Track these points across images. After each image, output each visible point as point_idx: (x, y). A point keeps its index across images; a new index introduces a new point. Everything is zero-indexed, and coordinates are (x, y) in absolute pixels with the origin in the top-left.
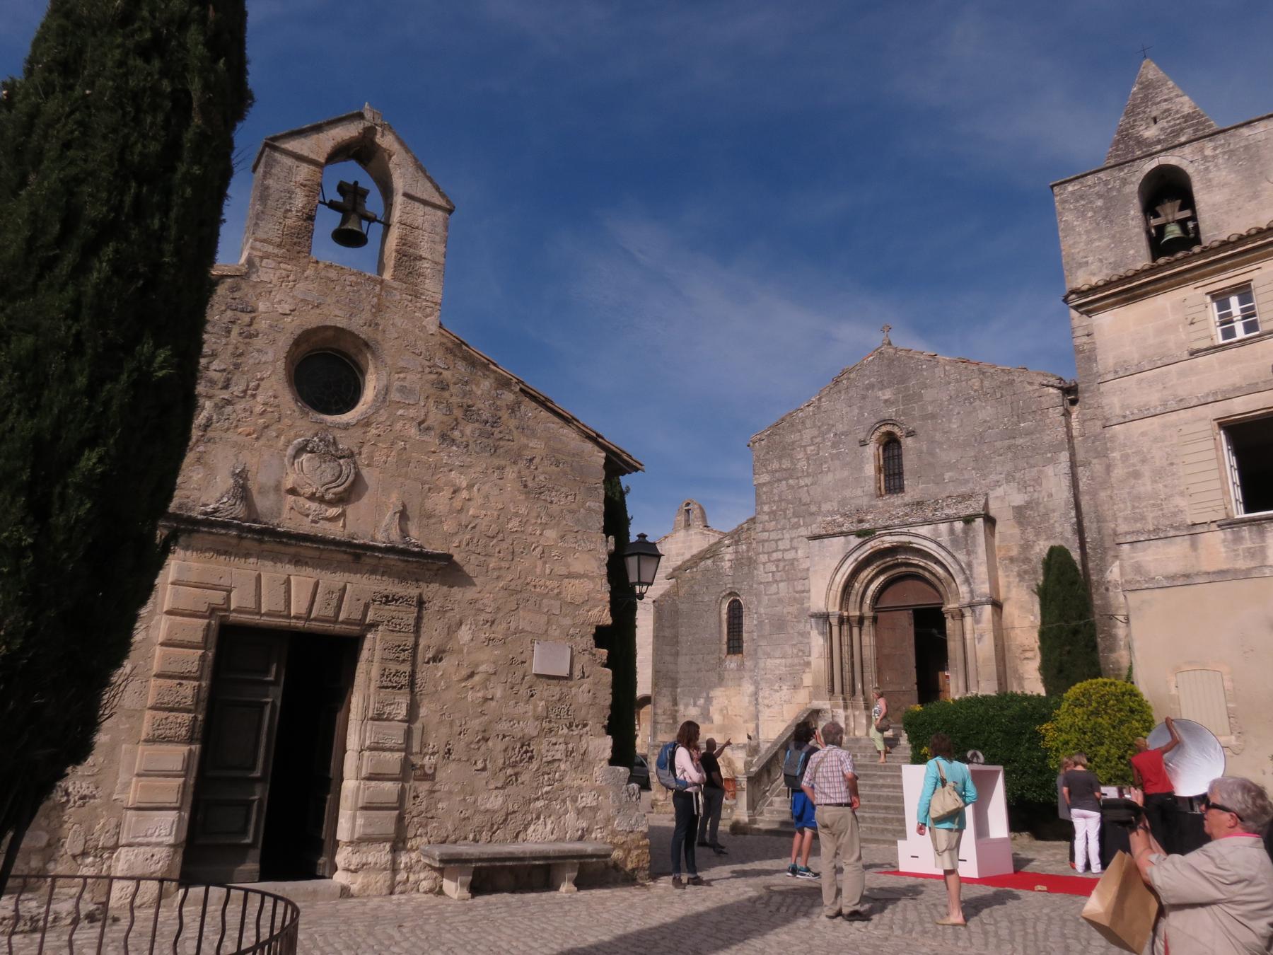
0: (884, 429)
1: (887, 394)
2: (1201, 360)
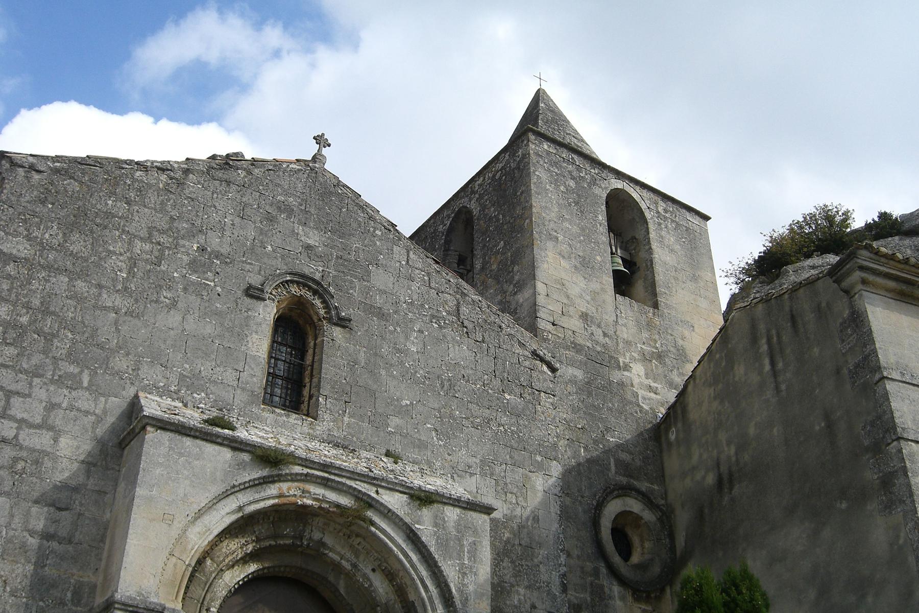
1: (314, 238)
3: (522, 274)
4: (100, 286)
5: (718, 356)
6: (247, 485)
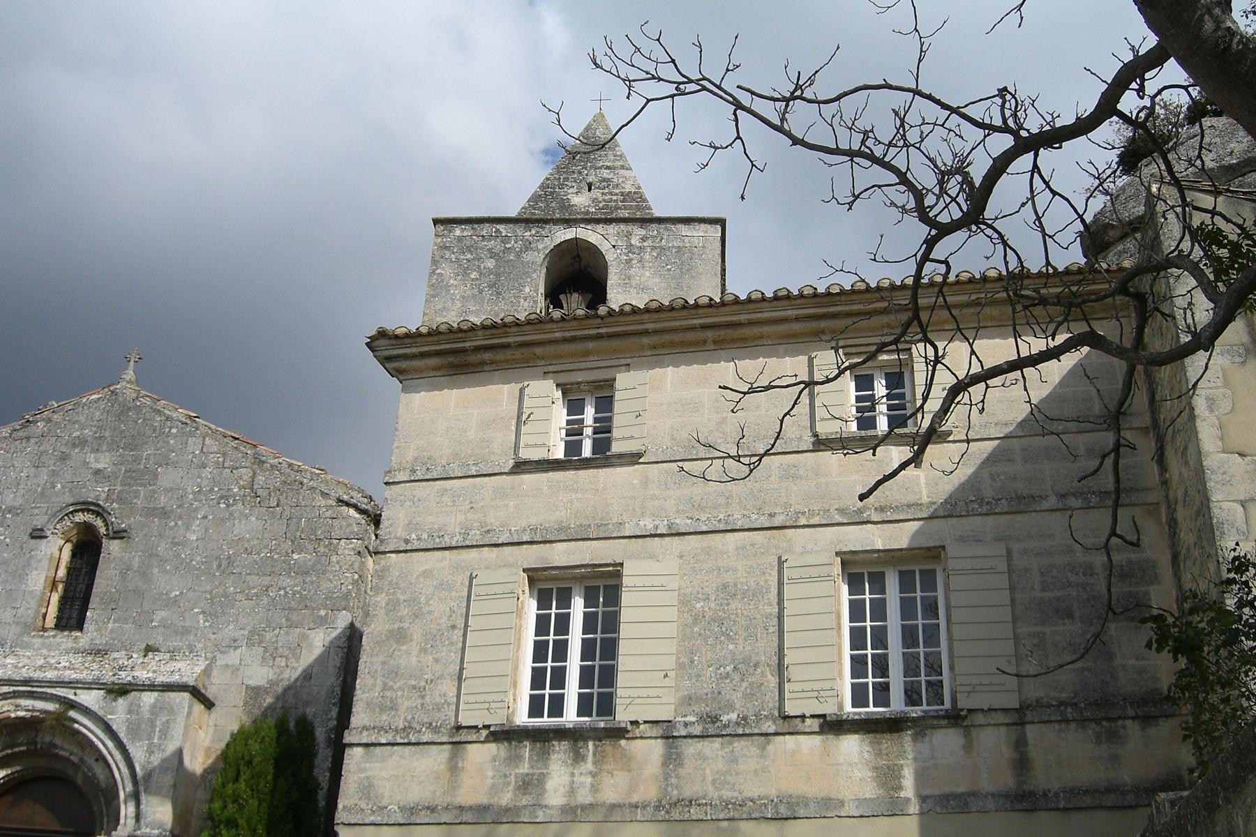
0: (80, 518)
1: (103, 461)
2: (529, 480)
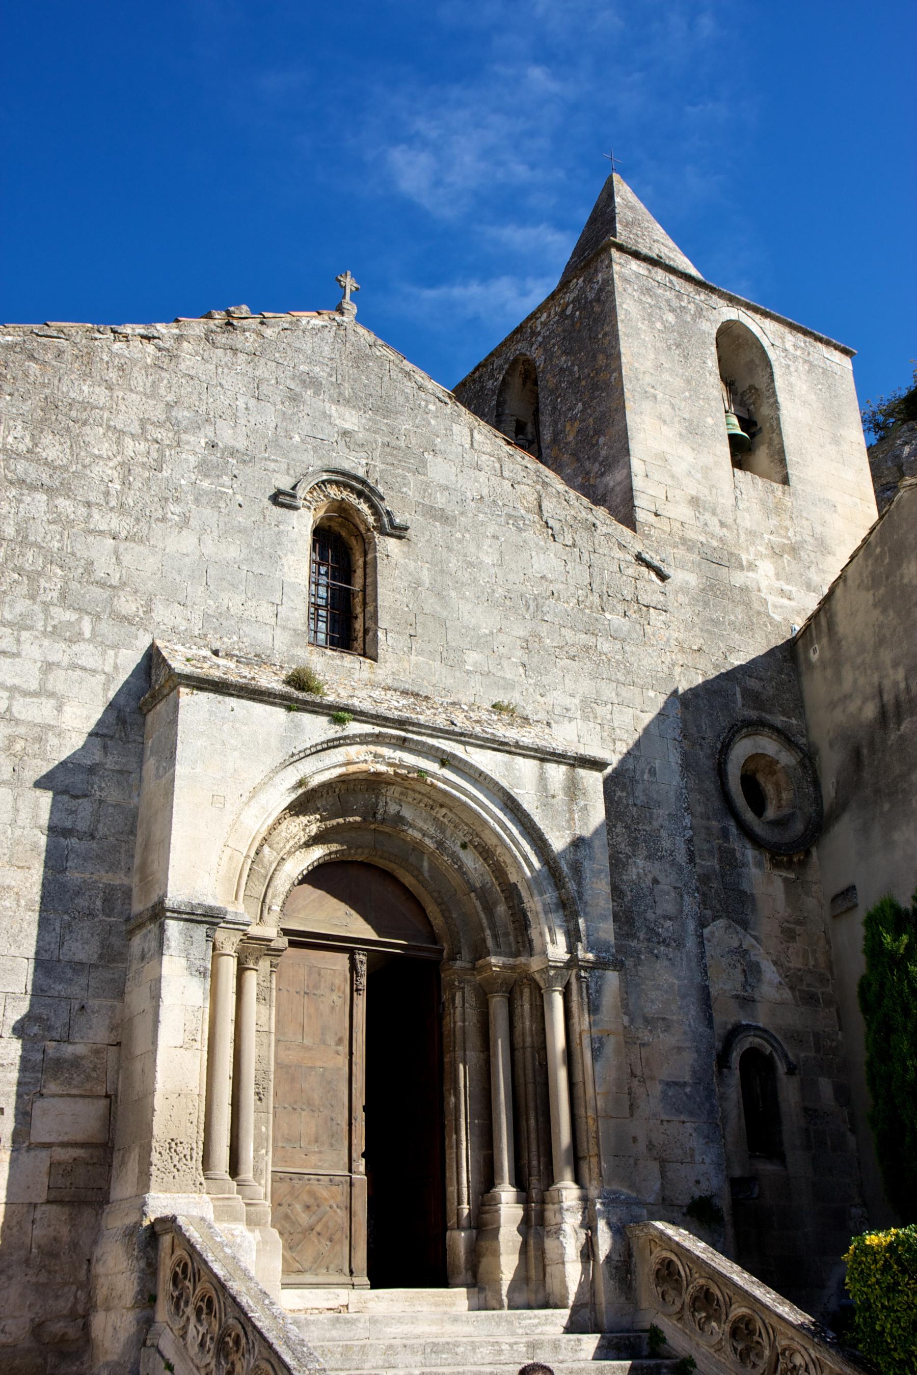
1: (351, 420)
3: (611, 448)
4: (89, 505)
5: (878, 550)
6: (308, 752)
